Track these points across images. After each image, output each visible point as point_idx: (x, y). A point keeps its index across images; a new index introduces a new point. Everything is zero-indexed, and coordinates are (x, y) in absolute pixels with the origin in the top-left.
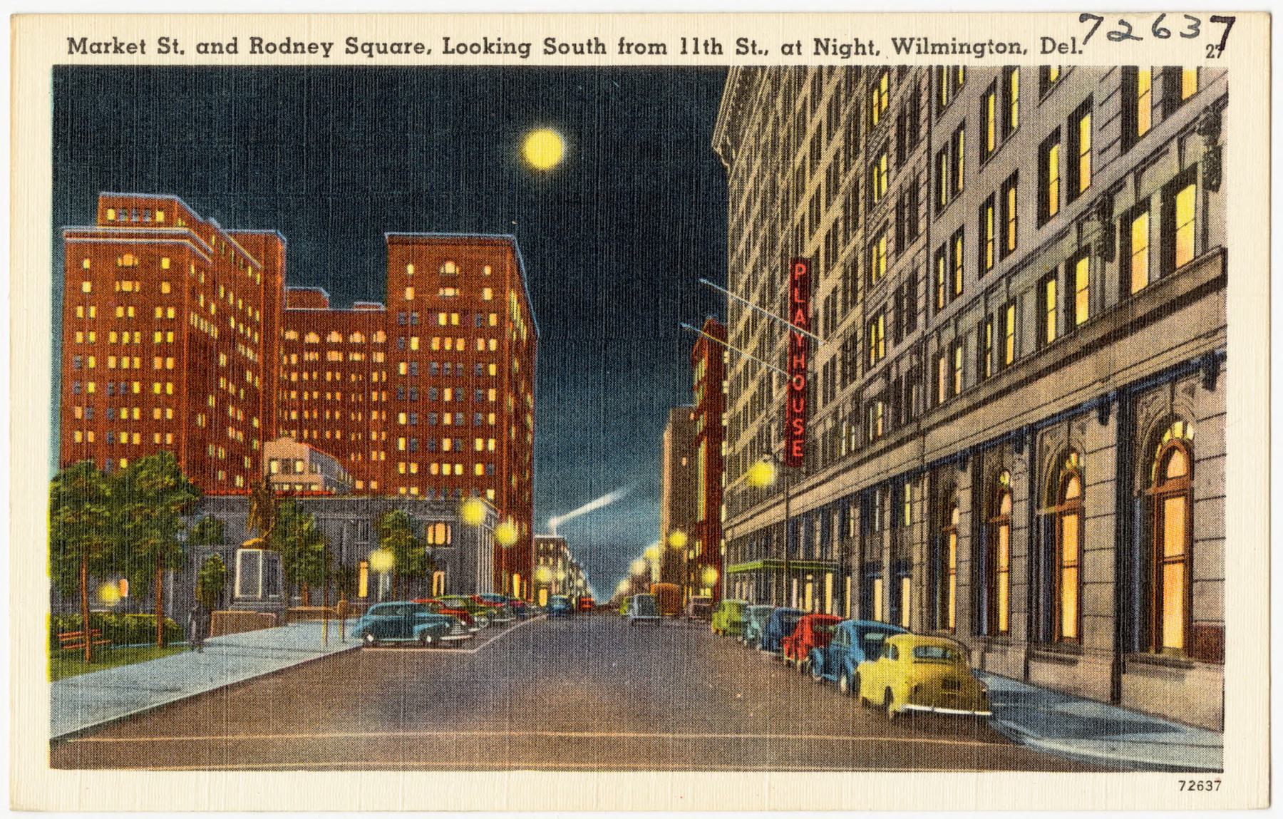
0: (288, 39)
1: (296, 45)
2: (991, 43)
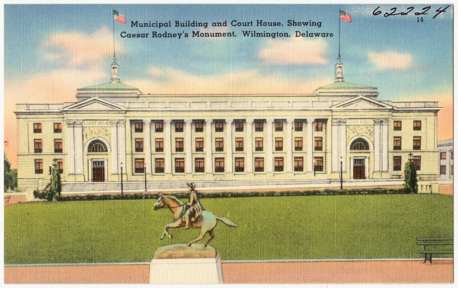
2: (278, 33)
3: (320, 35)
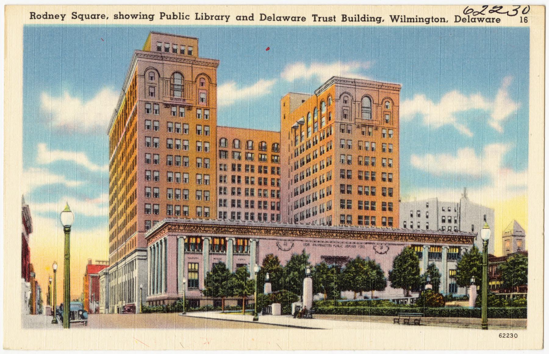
0: (46, 13)
1: (50, 15)
2: (432, 18)
3: (290, 19)
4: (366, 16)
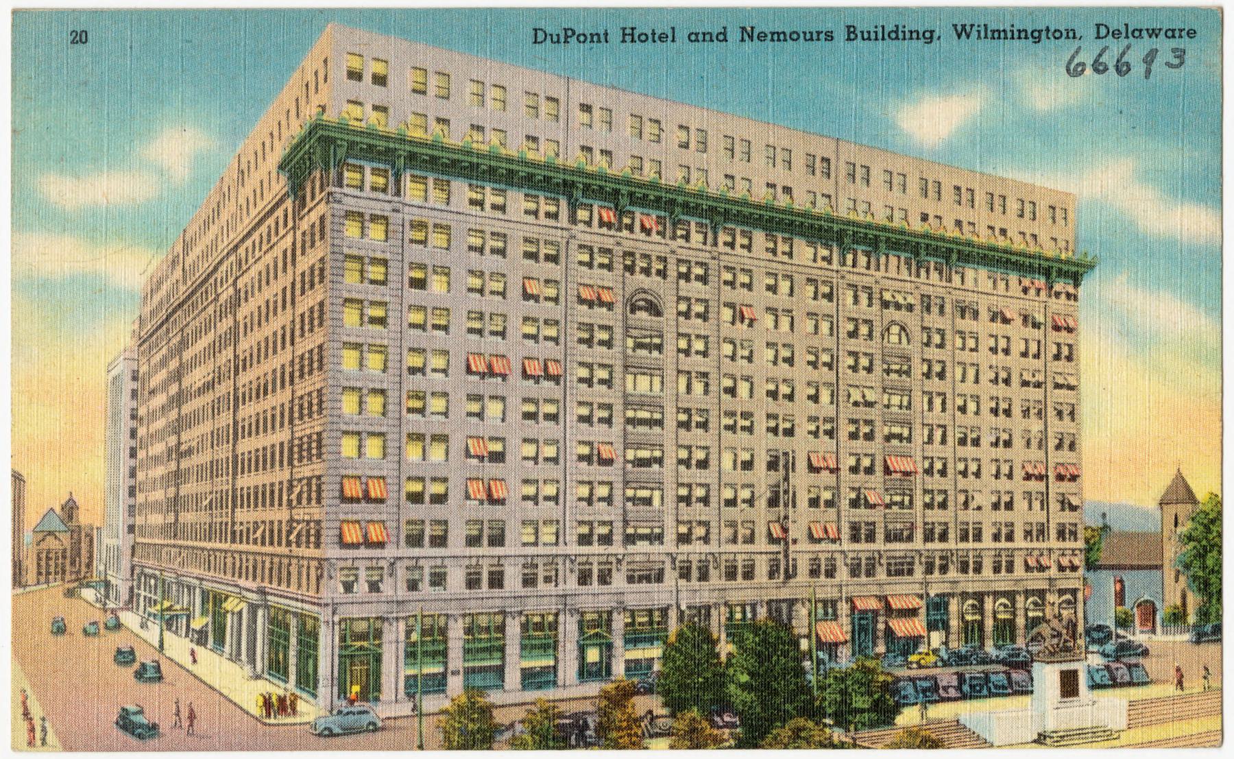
0: (897, 26)
3: (1163, 33)
4: (901, 29)
